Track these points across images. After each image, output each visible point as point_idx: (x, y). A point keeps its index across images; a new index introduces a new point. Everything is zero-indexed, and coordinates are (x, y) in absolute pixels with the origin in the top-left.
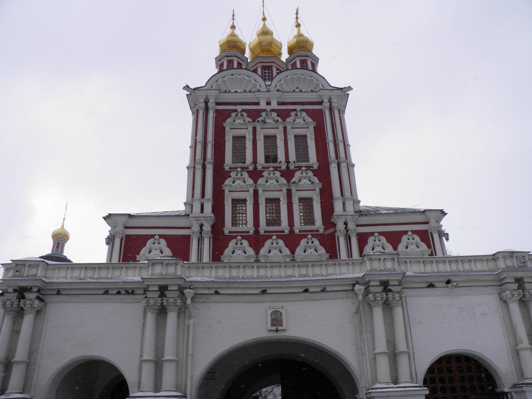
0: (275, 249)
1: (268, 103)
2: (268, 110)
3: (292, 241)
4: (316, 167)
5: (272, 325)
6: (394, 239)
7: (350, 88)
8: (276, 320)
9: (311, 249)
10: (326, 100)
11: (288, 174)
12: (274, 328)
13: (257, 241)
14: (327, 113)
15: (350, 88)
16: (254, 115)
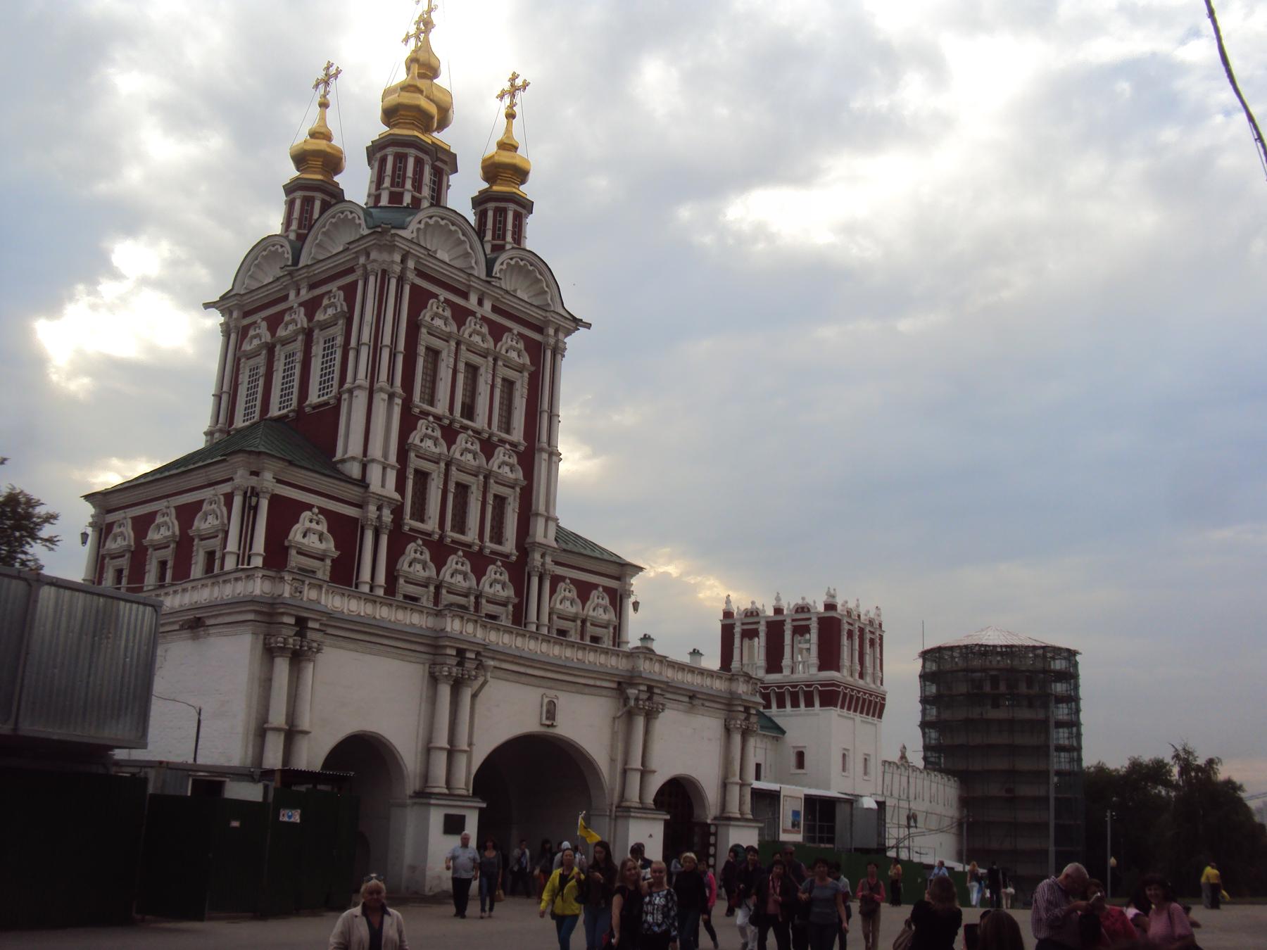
0: (456, 572)
1: (480, 303)
2: (479, 316)
3: (479, 562)
4: (522, 448)
5: (547, 718)
6: (584, 590)
7: (588, 326)
8: (551, 713)
9: (496, 584)
10: (551, 331)
11: (488, 448)
12: (548, 723)
13: (440, 551)
14: (549, 353)
15: (588, 326)
16: (461, 315)
